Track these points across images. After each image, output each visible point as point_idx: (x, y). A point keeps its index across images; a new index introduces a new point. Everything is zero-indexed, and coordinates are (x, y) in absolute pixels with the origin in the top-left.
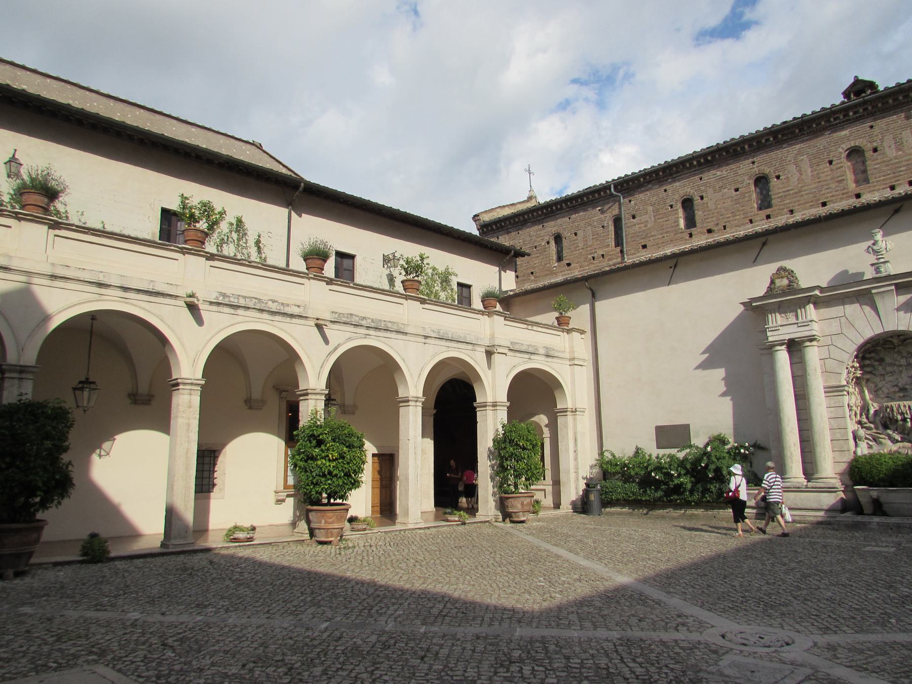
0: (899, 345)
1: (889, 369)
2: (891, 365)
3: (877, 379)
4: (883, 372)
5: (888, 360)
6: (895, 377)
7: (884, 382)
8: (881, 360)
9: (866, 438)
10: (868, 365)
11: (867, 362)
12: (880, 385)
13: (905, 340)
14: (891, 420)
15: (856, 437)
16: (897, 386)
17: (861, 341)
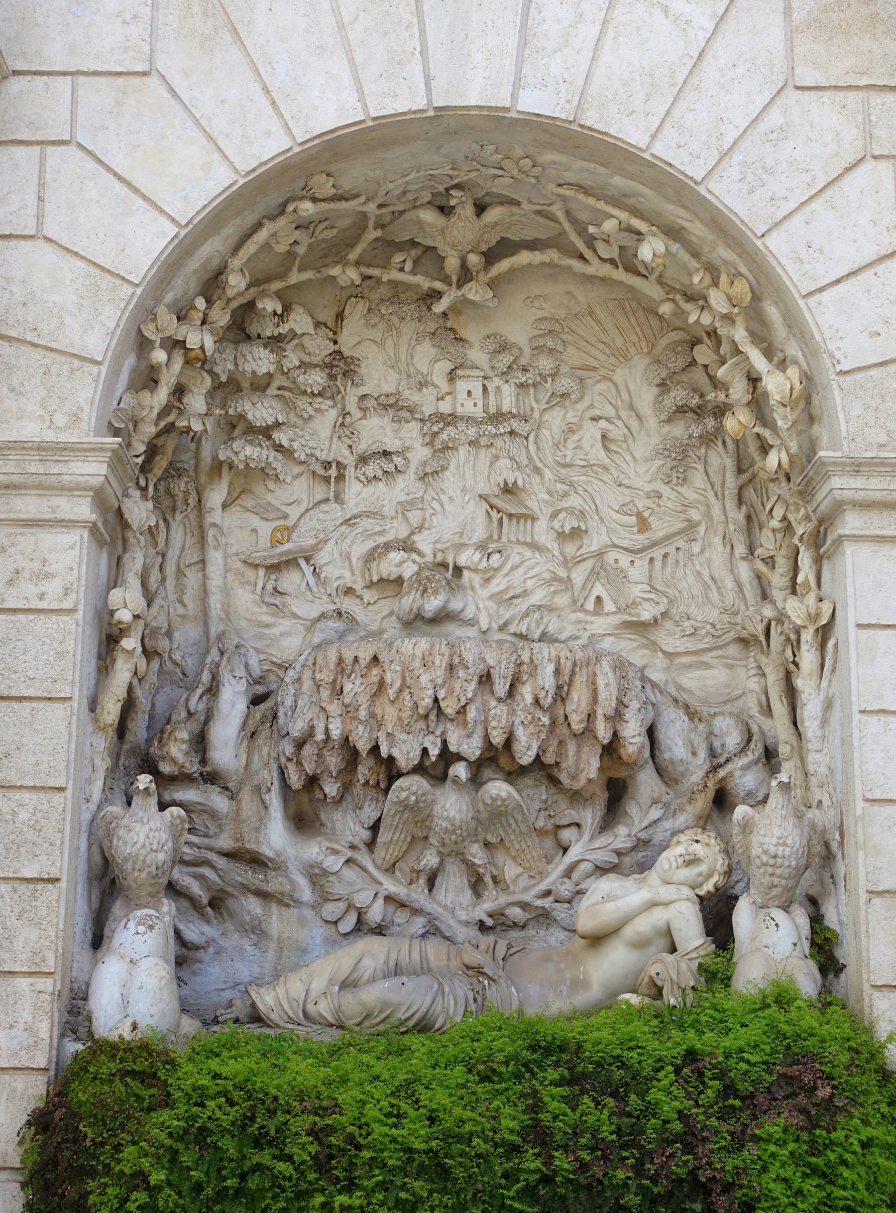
0: (466, 275)
1: (376, 431)
2: (394, 407)
3: (295, 492)
4: (340, 451)
5: (378, 375)
6: (405, 486)
7: (335, 512)
8: (340, 366)
9: (173, 890)
10: (260, 385)
11: (259, 361)
12: (303, 539)
13: (504, 248)
14: (352, 755)
15: (107, 887)
16: (407, 546)
17: (265, 144)
